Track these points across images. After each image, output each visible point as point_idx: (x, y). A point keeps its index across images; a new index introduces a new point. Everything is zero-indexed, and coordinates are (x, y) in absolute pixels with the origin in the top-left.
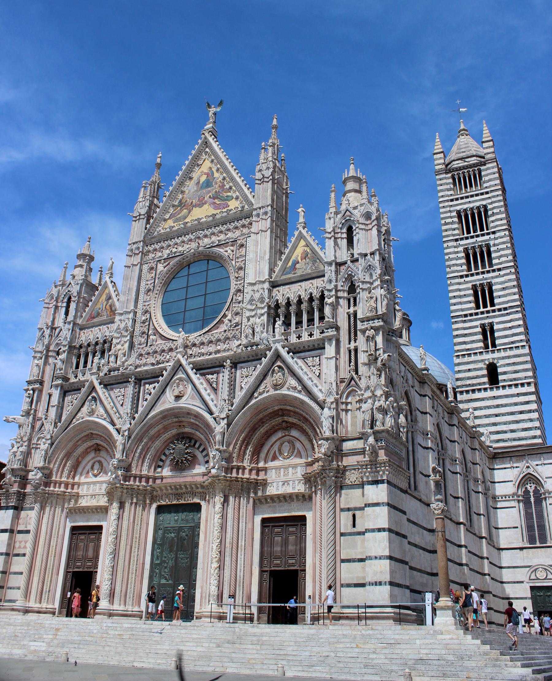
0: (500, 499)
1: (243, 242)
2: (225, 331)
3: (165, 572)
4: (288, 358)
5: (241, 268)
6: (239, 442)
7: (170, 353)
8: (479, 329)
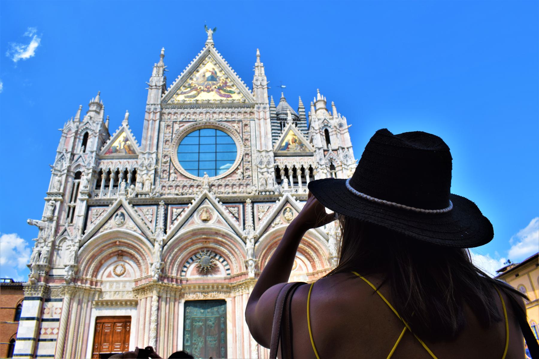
1: (248, 123)
2: (239, 179)
3: (196, 352)
5: (247, 140)
7: (191, 188)
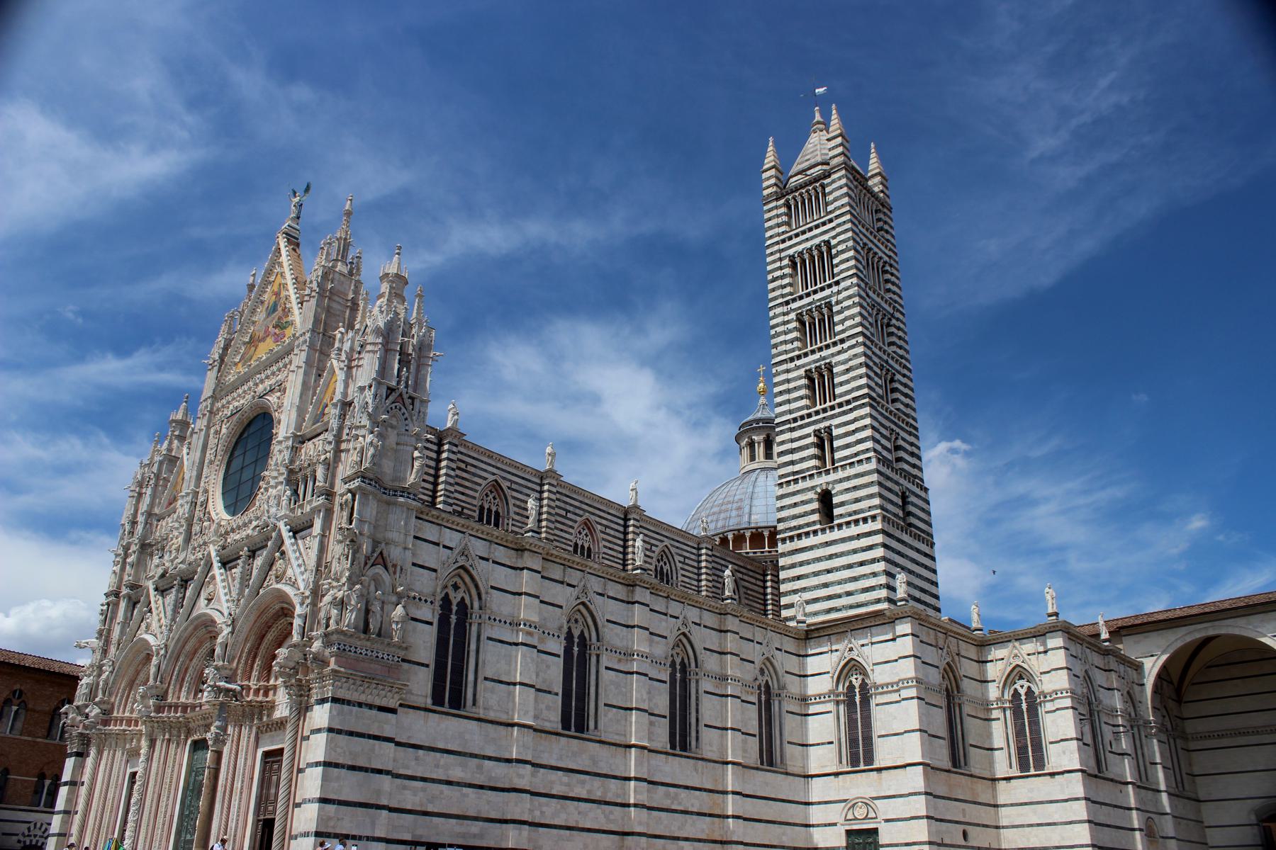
0: (813, 701)
4: (288, 542)
6: (244, 655)
8: (812, 439)
